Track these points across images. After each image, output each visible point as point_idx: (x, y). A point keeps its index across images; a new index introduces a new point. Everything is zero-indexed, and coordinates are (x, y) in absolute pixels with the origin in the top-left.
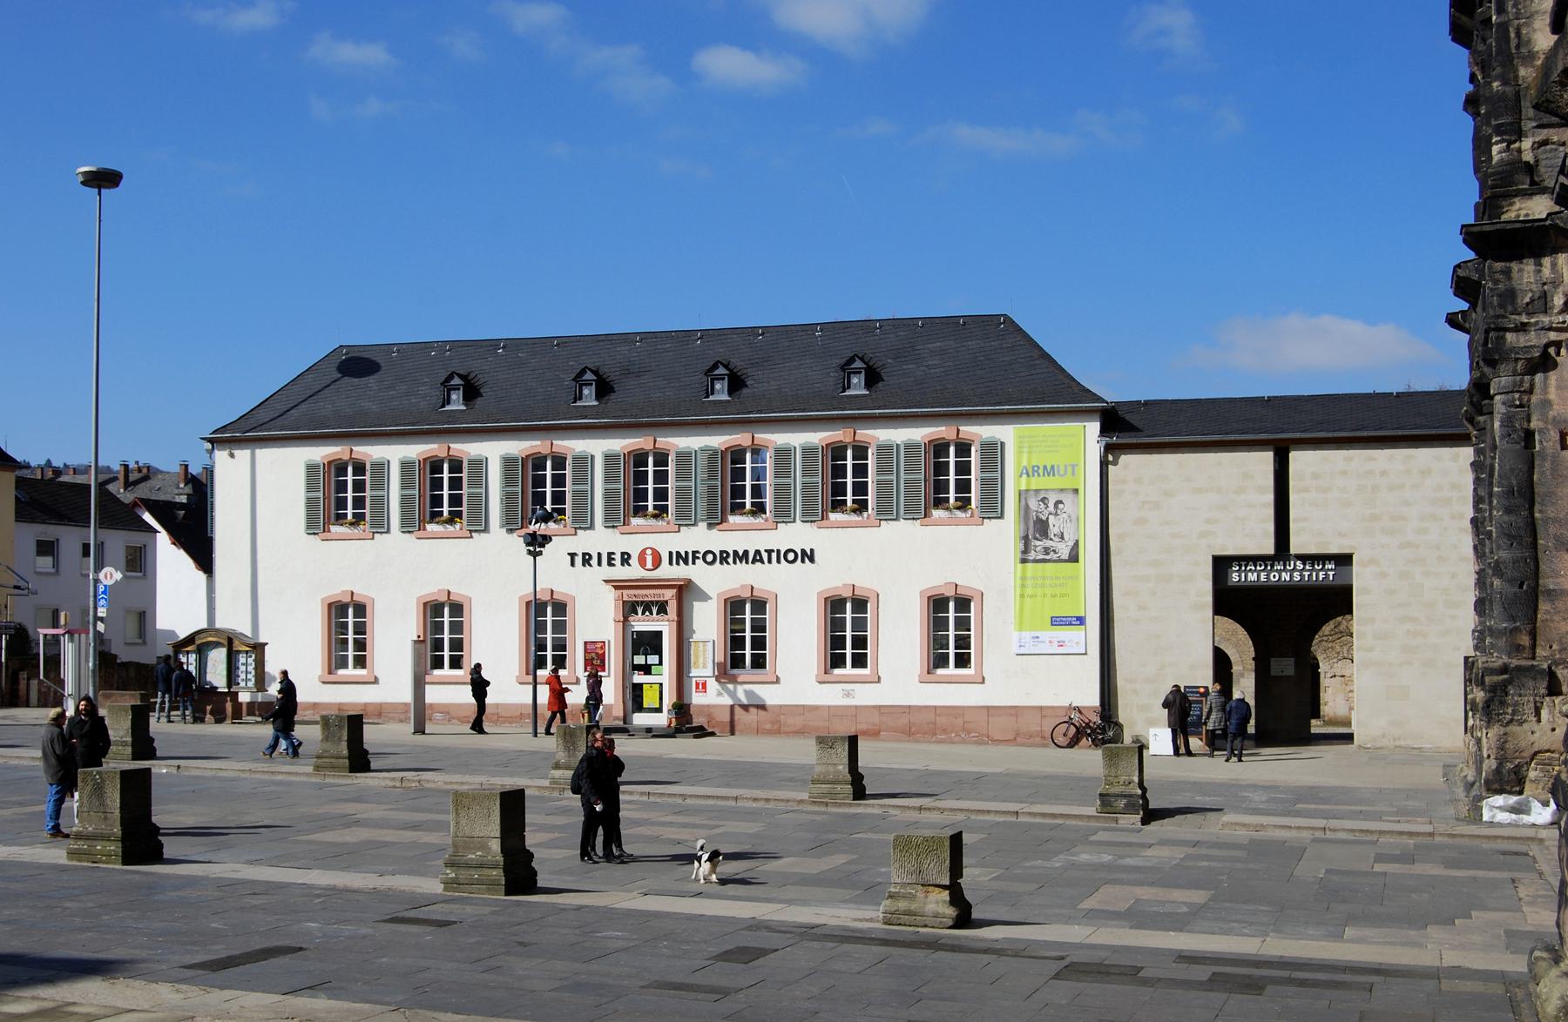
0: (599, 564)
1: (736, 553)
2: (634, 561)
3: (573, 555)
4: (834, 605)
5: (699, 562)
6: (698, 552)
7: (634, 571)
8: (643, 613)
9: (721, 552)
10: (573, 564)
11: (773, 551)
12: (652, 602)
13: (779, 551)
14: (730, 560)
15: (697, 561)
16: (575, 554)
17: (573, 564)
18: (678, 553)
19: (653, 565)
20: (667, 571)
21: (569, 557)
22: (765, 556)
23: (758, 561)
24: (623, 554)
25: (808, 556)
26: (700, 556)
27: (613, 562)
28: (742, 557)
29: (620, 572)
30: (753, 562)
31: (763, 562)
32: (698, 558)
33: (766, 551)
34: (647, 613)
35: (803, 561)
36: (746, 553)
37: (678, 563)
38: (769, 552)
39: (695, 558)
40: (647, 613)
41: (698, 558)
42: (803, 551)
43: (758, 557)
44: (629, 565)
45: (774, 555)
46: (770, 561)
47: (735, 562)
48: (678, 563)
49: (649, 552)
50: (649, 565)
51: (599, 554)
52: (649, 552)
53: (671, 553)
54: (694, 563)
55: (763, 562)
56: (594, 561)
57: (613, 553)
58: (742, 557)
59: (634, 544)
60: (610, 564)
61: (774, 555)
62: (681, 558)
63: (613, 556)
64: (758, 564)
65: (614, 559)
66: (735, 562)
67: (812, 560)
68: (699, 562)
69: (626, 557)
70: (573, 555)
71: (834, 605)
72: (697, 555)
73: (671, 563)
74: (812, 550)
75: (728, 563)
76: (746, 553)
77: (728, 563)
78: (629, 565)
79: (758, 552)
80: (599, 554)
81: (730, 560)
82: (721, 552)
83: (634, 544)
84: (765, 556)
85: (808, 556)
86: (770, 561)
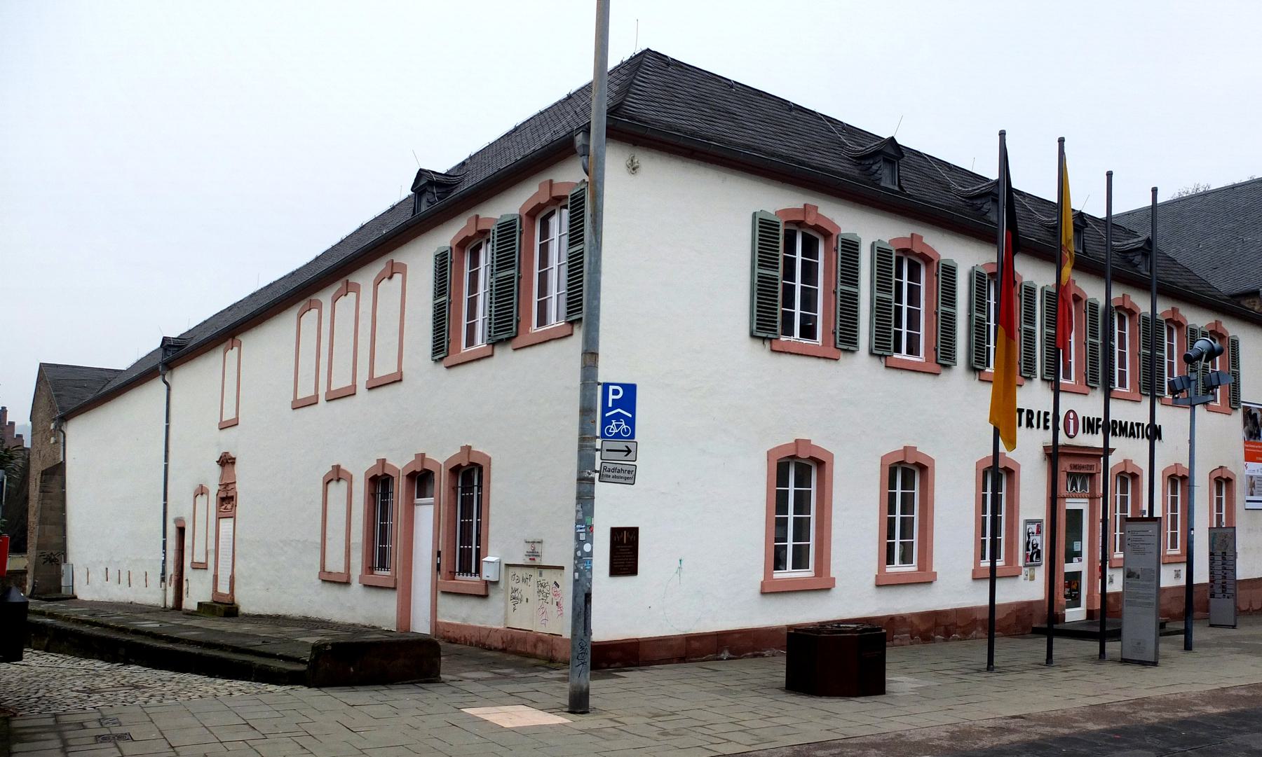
0: (1038, 427)
13: (1143, 424)
14: (1117, 430)
16: (1023, 410)
36: (1126, 423)
38: (1138, 425)
46: (1138, 437)
49: (1072, 415)
50: (1072, 433)
51: (1039, 412)
52: (1072, 415)
53: (1084, 418)
55: (1134, 437)
56: (1035, 422)
61: (1140, 428)
73: (1084, 432)
74: (1160, 426)
76: (1126, 423)
79: (1132, 423)
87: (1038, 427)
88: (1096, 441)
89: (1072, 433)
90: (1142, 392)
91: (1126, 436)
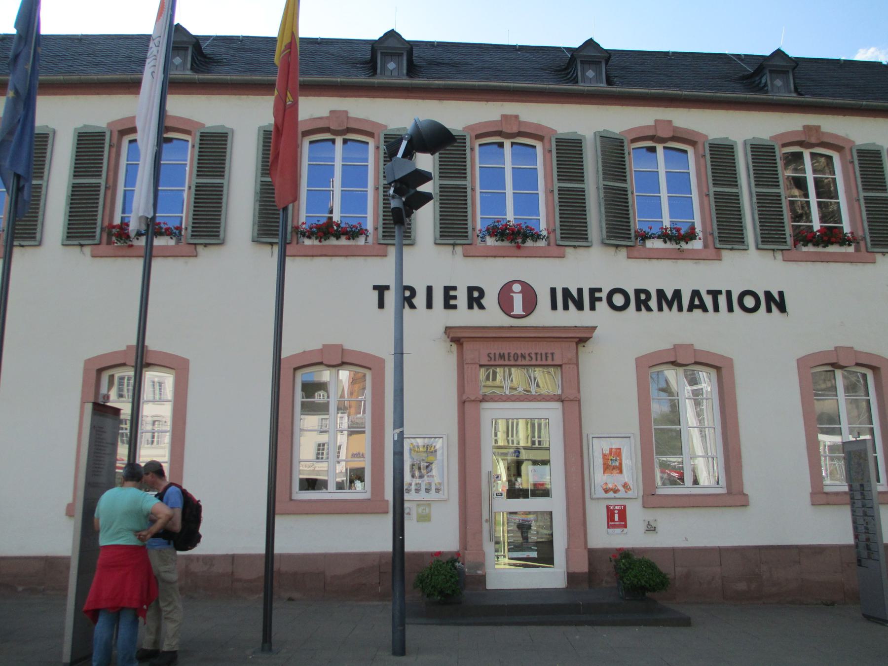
0: (429, 305)
1: (661, 293)
2: (491, 300)
3: (381, 290)
5: (602, 306)
6: (600, 290)
10: (381, 305)
11: (720, 292)
13: (729, 293)
14: (653, 303)
15: (597, 304)
17: (381, 305)
18: (566, 292)
19: (524, 311)
21: (376, 293)
22: (708, 300)
23: (697, 307)
24: (471, 290)
26: (604, 295)
27: (452, 302)
30: (691, 307)
31: (705, 310)
32: (600, 299)
35: (769, 310)
36: (677, 294)
37: (566, 307)
38: (715, 294)
39: (594, 301)
41: (600, 299)
42: (768, 294)
43: (697, 303)
44: (481, 307)
45: (722, 300)
46: (716, 309)
47: (660, 309)
48: (566, 307)
49: (517, 288)
50: (518, 309)
51: (429, 289)
52: (517, 288)
53: (553, 291)
54: (593, 308)
55: (705, 310)
56: (420, 300)
57: (454, 288)
60: (448, 306)
61: (722, 300)
63: (452, 293)
64: (698, 312)
65: (455, 297)
66: (660, 309)
67: (782, 308)
68: (602, 306)
69: (475, 298)
70: (381, 290)
72: (597, 295)
73: (554, 307)
74: (781, 294)
75: (649, 309)
76: (677, 294)
77: (649, 309)
78: (481, 307)
79: (696, 293)
80: (429, 289)
81: (653, 303)
82: (638, 292)
84: (708, 300)
87: (429, 305)
88: (571, 318)
89: (518, 309)
90: (719, 246)
91: (680, 309)
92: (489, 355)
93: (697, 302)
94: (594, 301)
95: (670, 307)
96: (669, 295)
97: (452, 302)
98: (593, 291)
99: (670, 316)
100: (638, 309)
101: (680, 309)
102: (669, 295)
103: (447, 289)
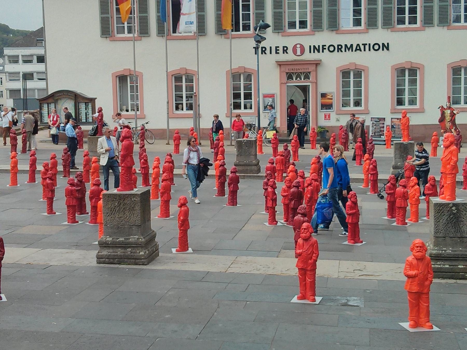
2: (290, 51)
4: (401, 71)
5: (326, 51)
6: (325, 46)
7: (290, 56)
8: (296, 79)
9: (338, 46)
11: (366, 44)
12: (301, 73)
13: (369, 44)
15: (324, 50)
19: (301, 53)
20: (308, 56)
21: (254, 49)
22: (362, 47)
23: (358, 50)
24: (284, 47)
25: (386, 47)
26: (327, 47)
27: (278, 52)
28: (349, 48)
29: (282, 57)
30: (355, 51)
31: (361, 51)
32: (325, 49)
33: (363, 44)
34: (298, 79)
36: (352, 46)
38: (365, 45)
39: (323, 49)
40: (298, 79)
41: (325, 49)
43: (358, 48)
44: (287, 53)
45: (367, 47)
47: (345, 51)
49: (298, 46)
50: (299, 53)
52: (298, 46)
53: (310, 46)
54: (323, 52)
55: (361, 51)
56: (268, 51)
57: (278, 47)
58: (349, 48)
59: (290, 42)
60: (277, 53)
61: (367, 47)
62: (316, 49)
63: (278, 49)
64: (359, 51)
65: (279, 50)
66: (345, 51)
67: (388, 49)
68: (326, 51)
69: (285, 50)
71: (401, 71)
72: (324, 47)
73: (310, 52)
74: (388, 44)
75: (342, 51)
76: (352, 46)
77: (342, 51)
78: (287, 53)
79: (358, 45)
81: (343, 49)
83: (290, 42)
84: (362, 47)
85: (386, 47)
86: (365, 50)
89: (299, 53)
91: (352, 51)
92: (289, 69)
93: (358, 48)
94: (323, 49)
95: (349, 50)
96: (349, 47)
97: (278, 52)
98: (323, 46)
99: (349, 53)
100: (338, 51)
101: (352, 51)
102: (349, 47)
103: (276, 47)
